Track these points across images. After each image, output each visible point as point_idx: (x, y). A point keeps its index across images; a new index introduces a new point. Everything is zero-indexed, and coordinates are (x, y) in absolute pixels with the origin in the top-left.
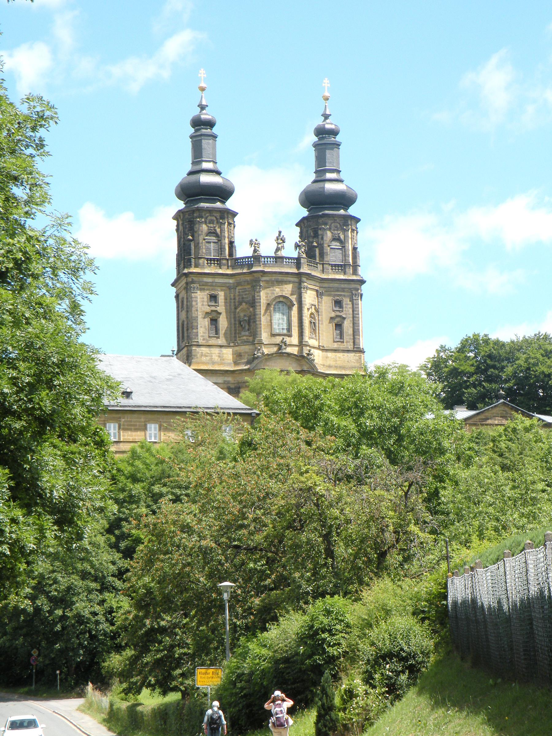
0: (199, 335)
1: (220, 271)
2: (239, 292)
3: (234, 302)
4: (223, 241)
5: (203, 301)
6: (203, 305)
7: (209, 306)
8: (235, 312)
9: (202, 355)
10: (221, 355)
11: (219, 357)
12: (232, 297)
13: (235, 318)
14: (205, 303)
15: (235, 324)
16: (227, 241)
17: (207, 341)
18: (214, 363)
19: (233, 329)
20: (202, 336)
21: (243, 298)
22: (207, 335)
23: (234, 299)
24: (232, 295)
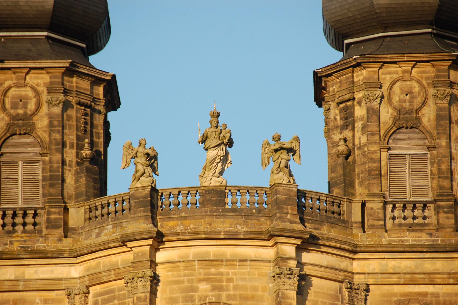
1: (40, 245)
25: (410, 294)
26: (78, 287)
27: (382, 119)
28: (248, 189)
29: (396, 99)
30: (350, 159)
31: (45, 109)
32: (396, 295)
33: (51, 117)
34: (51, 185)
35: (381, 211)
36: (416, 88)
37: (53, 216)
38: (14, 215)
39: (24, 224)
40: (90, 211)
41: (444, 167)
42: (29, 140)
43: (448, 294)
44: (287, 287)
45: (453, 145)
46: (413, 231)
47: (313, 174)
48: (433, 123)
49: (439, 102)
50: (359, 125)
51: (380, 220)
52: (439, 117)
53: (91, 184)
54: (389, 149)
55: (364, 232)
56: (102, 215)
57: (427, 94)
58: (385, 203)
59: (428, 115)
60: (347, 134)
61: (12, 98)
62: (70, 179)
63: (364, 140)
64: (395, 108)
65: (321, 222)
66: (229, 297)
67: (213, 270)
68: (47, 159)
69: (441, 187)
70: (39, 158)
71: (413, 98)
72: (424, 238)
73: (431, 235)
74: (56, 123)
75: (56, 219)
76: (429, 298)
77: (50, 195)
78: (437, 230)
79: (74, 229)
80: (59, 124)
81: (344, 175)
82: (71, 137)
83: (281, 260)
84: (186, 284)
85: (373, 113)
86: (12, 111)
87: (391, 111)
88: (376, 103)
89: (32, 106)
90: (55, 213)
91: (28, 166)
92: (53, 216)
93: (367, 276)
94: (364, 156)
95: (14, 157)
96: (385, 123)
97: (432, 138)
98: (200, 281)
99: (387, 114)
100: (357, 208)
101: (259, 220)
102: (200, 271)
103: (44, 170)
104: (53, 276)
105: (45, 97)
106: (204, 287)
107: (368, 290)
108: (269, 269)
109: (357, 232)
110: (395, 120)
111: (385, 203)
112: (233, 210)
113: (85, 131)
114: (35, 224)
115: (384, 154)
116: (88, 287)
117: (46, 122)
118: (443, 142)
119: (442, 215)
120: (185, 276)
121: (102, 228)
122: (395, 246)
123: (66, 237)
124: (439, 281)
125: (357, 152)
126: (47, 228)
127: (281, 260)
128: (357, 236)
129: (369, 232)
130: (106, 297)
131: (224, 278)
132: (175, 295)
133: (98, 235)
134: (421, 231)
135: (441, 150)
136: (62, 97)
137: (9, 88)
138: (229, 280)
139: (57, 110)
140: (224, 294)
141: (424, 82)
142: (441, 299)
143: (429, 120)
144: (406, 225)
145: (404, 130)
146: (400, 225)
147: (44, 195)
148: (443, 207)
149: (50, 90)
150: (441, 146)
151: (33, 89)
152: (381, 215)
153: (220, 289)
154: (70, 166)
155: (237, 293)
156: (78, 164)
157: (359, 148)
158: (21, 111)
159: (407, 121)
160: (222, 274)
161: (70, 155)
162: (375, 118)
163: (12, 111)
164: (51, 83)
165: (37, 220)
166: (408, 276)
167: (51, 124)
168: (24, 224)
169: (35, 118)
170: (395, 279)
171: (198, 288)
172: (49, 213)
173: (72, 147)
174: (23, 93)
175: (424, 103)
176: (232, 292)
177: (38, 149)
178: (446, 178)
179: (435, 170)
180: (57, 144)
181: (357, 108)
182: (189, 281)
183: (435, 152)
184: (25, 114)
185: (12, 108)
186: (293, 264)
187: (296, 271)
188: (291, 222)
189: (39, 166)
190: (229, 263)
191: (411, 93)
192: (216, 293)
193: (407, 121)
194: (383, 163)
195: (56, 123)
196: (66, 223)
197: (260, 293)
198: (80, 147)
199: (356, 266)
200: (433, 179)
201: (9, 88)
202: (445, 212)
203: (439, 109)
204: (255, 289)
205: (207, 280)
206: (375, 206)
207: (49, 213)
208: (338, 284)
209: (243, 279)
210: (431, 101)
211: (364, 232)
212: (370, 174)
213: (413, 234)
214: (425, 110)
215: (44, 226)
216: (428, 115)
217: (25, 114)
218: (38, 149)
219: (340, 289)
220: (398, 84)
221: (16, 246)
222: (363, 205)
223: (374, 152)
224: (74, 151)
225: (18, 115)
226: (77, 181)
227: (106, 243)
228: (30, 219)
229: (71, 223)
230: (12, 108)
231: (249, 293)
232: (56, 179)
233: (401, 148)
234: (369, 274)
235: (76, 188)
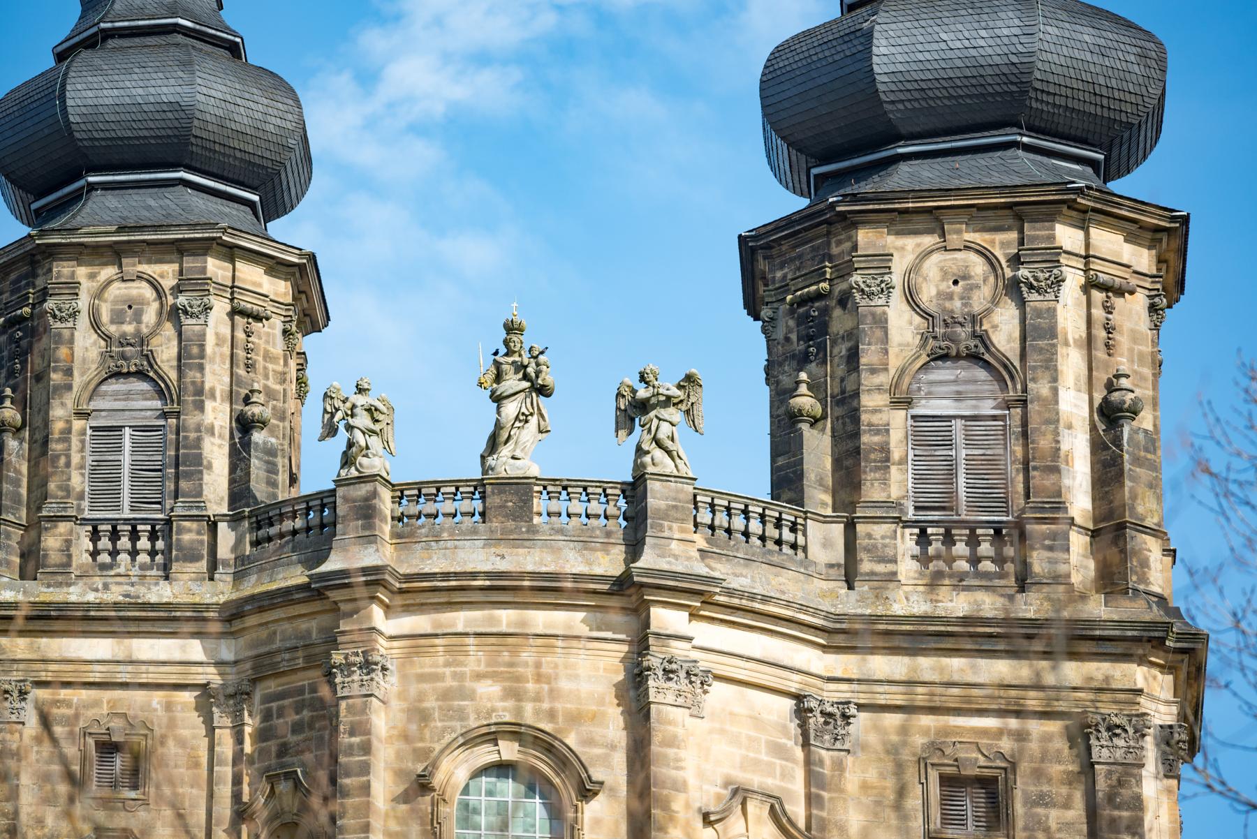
4: (191, 419)
16: (218, 415)
38: (115, 535)
39: (134, 553)
40: (259, 528)
61: (115, 302)
75: (192, 541)
86: (112, 329)
90: (190, 531)
137: (109, 282)
158: (129, 328)
168: (134, 553)
174: (134, 292)
184: (138, 333)
185: (112, 322)
201: (109, 282)
217: (138, 333)
225: (124, 335)
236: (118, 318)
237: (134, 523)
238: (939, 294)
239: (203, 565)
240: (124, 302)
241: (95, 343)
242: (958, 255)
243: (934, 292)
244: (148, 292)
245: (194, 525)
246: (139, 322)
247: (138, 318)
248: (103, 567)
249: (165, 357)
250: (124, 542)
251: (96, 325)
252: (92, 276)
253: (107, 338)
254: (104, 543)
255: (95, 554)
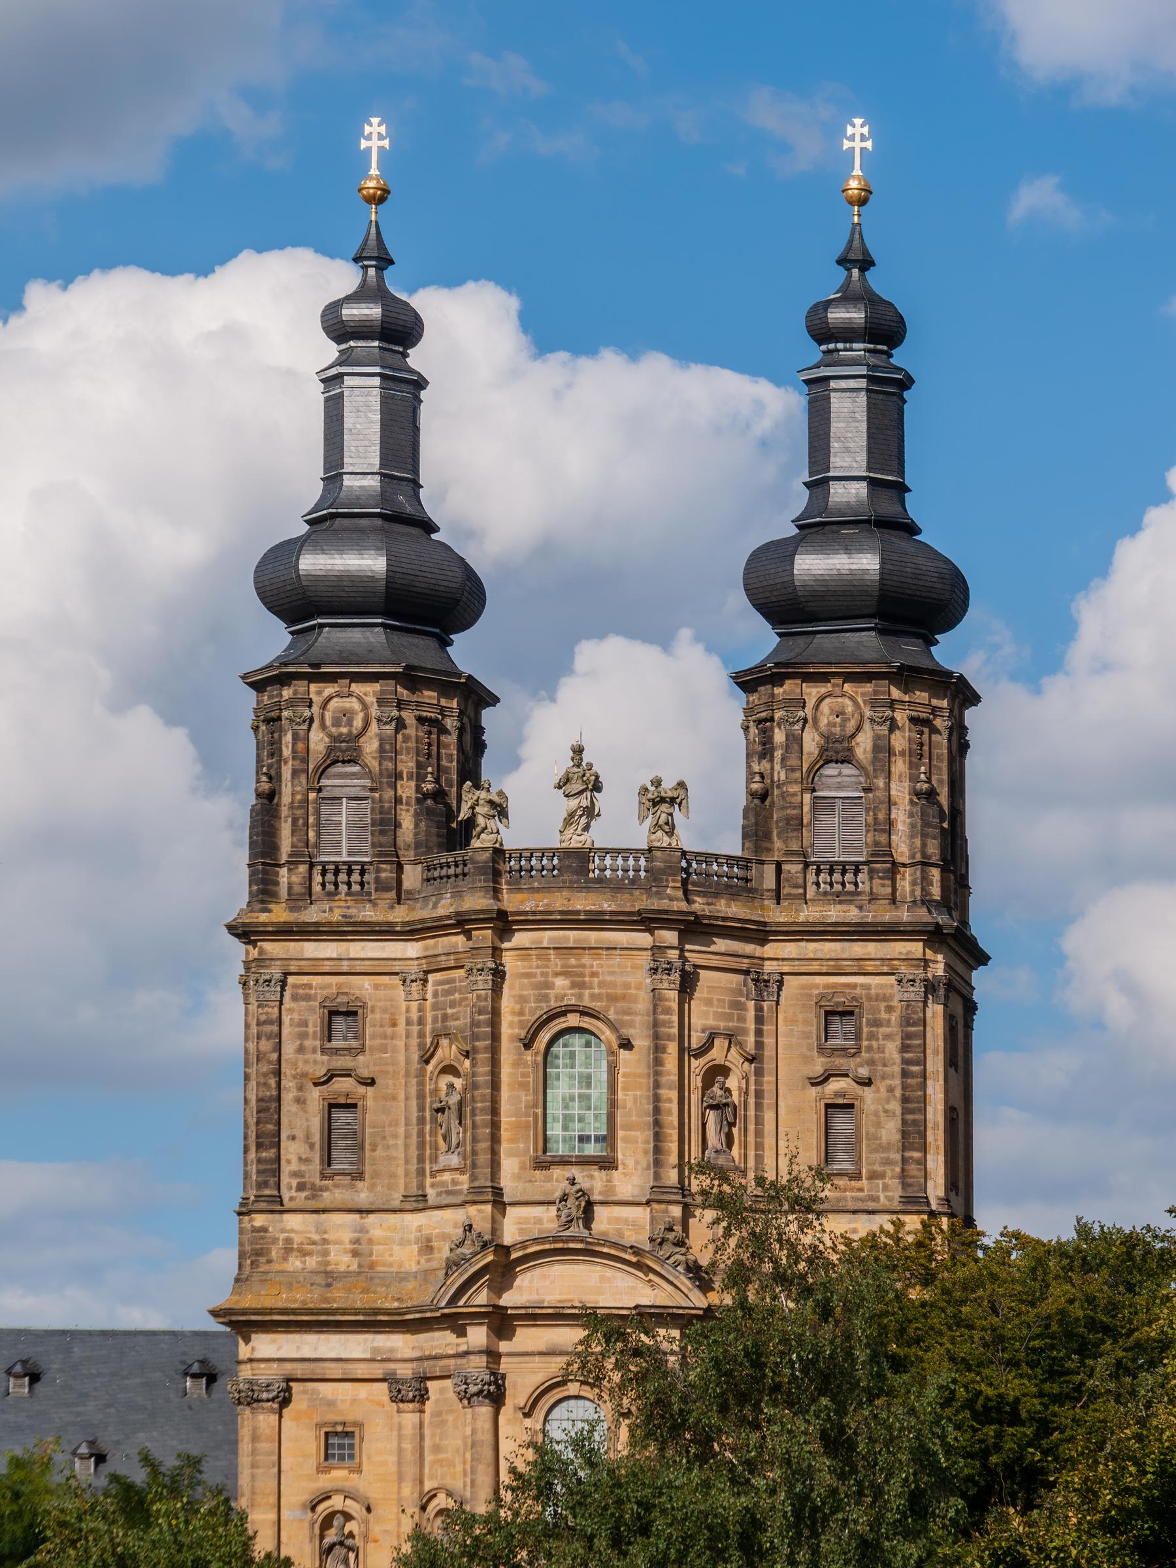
0: (286, 1169)
1: (368, 914)
2: (435, 995)
3: (421, 1035)
5: (303, 1036)
6: (301, 1050)
7: (324, 1051)
8: (421, 1074)
9: (288, 1250)
10: (364, 1247)
11: (355, 1254)
12: (415, 1016)
13: (421, 1096)
14: (312, 1043)
15: (421, 1121)
17: (316, 1191)
18: (329, 1277)
19: (414, 1139)
20: (295, 1174)
21: (445, 1017)
22: (316, 1165)
23: (421, 1021)
24: (414, 1006)
25: (835, 985)
26: (414, 969)
27: (806, 749)
28: (618, 851)
29: (823, 721)
30: (767, 803)
31: (374, 727)
32: (817, 986)
33: (382, 740)
34: (382, 832)
35: (801, 875)
36: (850, 709)
37: (383, 875)
38: (337, 872)
41: (881, 816)
42: (355, 769)
43: (881, 986)
44: (666, 985)
45: (893, 785)
46: (841, 902)
47: (713, 826)
48: (870, 755)
49: (876, 727)
50: (778, 754)
51: (799, 887)
52: (876, 748)
53: (434, 830)
54: (814, 790)
55: (778, 903)
56: (441, 878)
57: (862, 716)
58: (807, 865)
59: (863, 745)
60: (765, 765)
61: (334, 712)
62: (407, 822)
63: (783, 777)
64: (822, 735)
65: (716, 895)
66: (593, 997)
67: (573, 961)
68: (377, 795)
69: (876, 844)
70: (368, 794)
71: (846, 720)
72: (852, 914)
73: (861, 908)
74: (388, 747)
75: (387, 878)
76: (858, 991)
77: (381, 846)
78: (870, 901)
79: (409, 892)
80: (389, 750)
81: (756, 824)
82: (407, 764)
83: (658, 949)
84: (539, 979)
85: (795, 741)
86: (333, 730)
87: (817, 738)
88: (797, 727)
89: (358, 723)
90: (385, 870)
91: (353, 804)
92: (383, 875)
93: (780, 963)
94: (784, 798)
95: (337, 793)
96: (809, 754)
97: (867, 776)
98: (557, 974)
99: (811, 742)
100: (770, 870)
101: (632, 895)
102: (556, 963)
103: (373, 809)
104: (384, 955)
105: (374, 711)
106: (561, 982)
107: (780, 983)
108: (645, 959)
109: (769, 903)
110: (823, 750)
111: (807, 865)
112: (599, 880)
113: (429, 755)
114: (362, 884)
115: (807, 797)
116: (427, 972)
117: (375, 745)
118: (881, 783)
119: (876, 881)
120: (538, 967)
121: (440, 896)
122: (814, 924)
123: (399, 903)
124: (870, 969)
125: (776, 792)
126: (377, 890)
127: (658, 949)
128: (769, 909)
129: (784, 903)
130: (446, 987)
131: (587, 971)
132: (525, 993)
133: (435, 907)
134: (850, 902)
135: (878, 793)
136: (395, 713)
137: (330, 698)
138: (594, 975)
139: (389, 729)
140: (587, 992)
141: (860, 700)
142: (873, 991)
143: (865, 752)
144: (832, 894)
145: (833, 765)
146: (825, 893)
147: (373, 845)
148: (878, 871)
149: (381, 702)
150: (878, 788)
151: (359, 698)
152: (800, 881)
153: (581, 985)
154: (408, 804)
155: (603, 991)
156: (418, 801)
157: (778, 787)
158: (344, 730)
159: (837, 752)
160: (584, 966)
161: (407, 789)
162: (796, 747)
163: (333, 730)
164: (382, 692)
165: (366, 877)
166: (832, 963)
167: (381, 749)
168: (349, 884)
169: (362, 740)
170: (815, 966)
171: (553, 984)
172: (378, 871)
173: (410, 778)
174: (348, 705)
175: (859, 728)
176: (596, 991)
177: (367, 783)
178: (883, 831)
179: (870, 819)
180: (389, 776)
181: (777, 730)
182: (542, 973)
183: (870, 795)
184: (350, 732)
185: (333, 725)
186: (673, 954)
187: (678, 964)
188: (671, 899)
189: (367, 805)
190: (592, 951)
191: (843, 713)
192: (576, 991)
193: (837, 751)
194: (806, 809)
195: (388, 747)
196: (399, 882)
197: (633, 991)
198: (420, 778)
199: (769, 950)
200: (868, 831)
201: (330, 698)
202: (881, 878)
203: (877, 738)
204: (627, 986)
205: (565, 974)
206: (793, 869)
207: (378, 871)
208: (741, 977)
209: (612, 973)
210: (867, 726)
211: (778, 903)
212: (788, 824)
213: (839, 907)
214: (860, 738)
215: (373, 886)
216: (863, 745)
217: (350, 732)
218: (367, 783)
219: (745, 980)
220: (827, 701)
221: (336, 917)
222: (779, 866)
223: (794, 795)
224: (413, 784)
225: (341, 734)
226: (416, 825)
227: (440, 918)
228: (356, 877)
229: (407, 884)
230: (333, 725)
231: (619, 991)
232: (387, 824)
233: (829, 788)
234: (783, 959)
235: (416, 834)
236: (337, 723)
237: (349, 864)
238: (829, 723)
239: (393, 894)
240: (340, 712)
241: (322, 740)
242: (840, 700)
243: (826, 721)
244: (357, 706)
245: (388, 867)
246: (351, 726)
247: (350, 723)
248: (330, 894)
249: (368, 750)
250: (343, 877)
251: (323, 726)
252: (319, 693)
253: (330, 736)
254: (330, 877)
255: (323, 885)
